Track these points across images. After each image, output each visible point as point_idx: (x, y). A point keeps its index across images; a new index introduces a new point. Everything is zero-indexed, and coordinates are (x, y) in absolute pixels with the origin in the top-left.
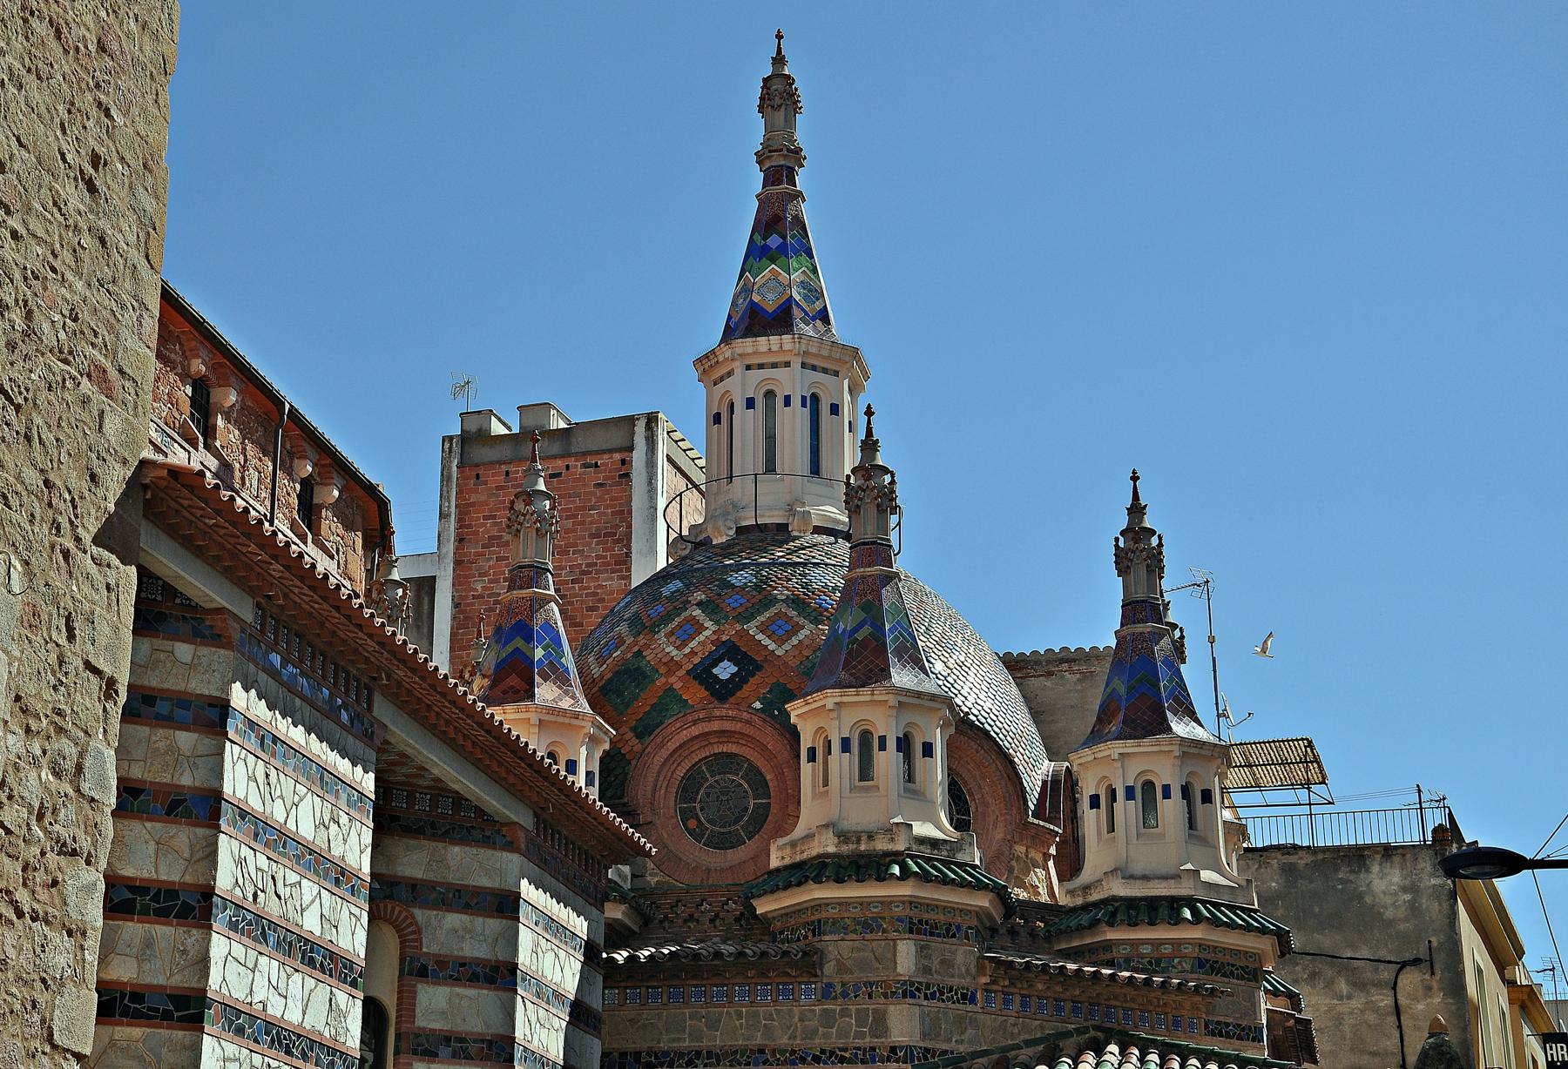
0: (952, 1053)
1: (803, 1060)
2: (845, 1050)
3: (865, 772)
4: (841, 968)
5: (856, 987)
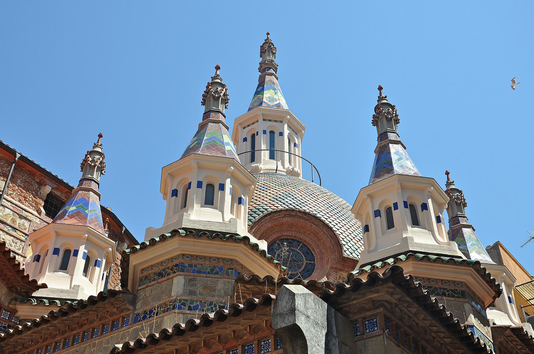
5: (151, 311)
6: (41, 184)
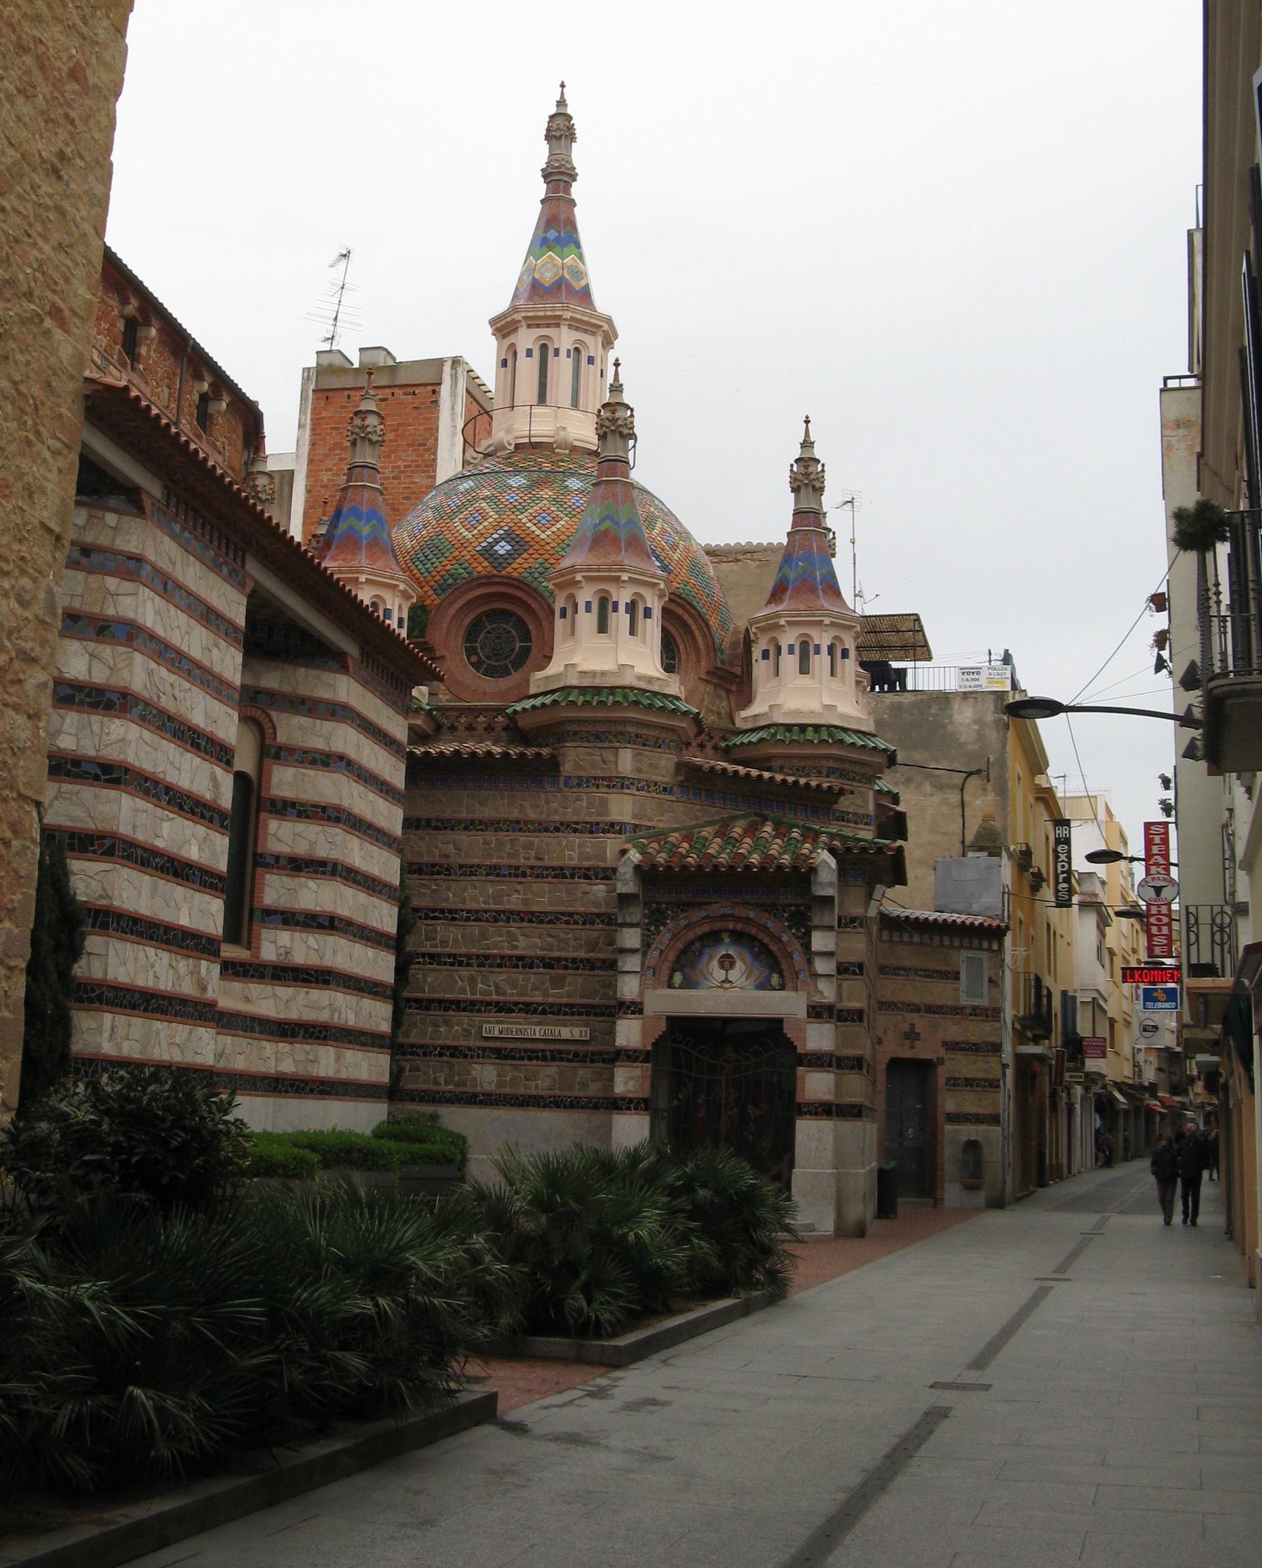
0: (654, 828)
1: (547, 830)
2: (577, 823)
3: (603, 628)
4: (577, 766)
6: (199, 378)
